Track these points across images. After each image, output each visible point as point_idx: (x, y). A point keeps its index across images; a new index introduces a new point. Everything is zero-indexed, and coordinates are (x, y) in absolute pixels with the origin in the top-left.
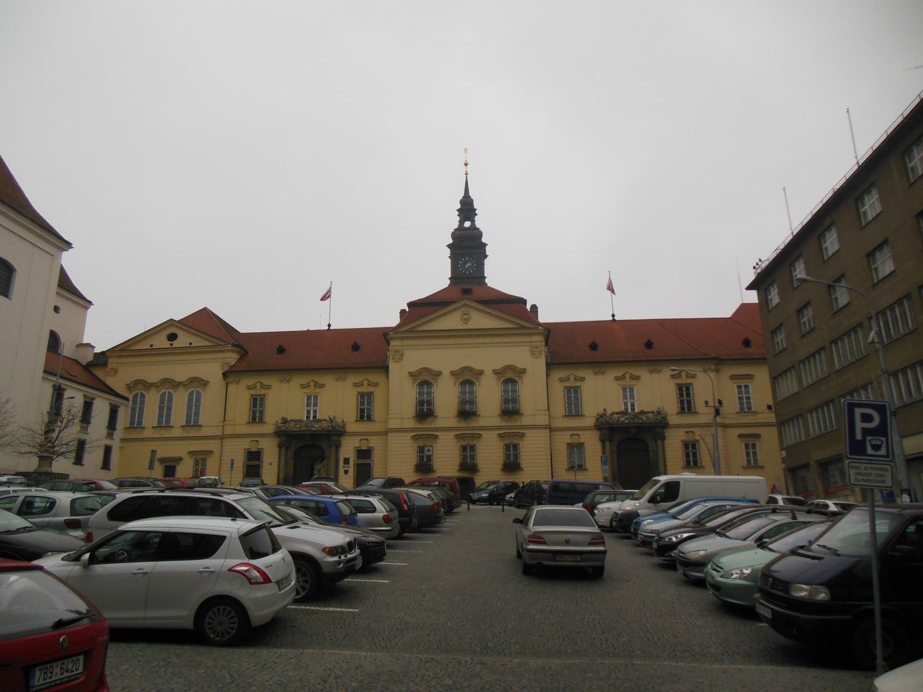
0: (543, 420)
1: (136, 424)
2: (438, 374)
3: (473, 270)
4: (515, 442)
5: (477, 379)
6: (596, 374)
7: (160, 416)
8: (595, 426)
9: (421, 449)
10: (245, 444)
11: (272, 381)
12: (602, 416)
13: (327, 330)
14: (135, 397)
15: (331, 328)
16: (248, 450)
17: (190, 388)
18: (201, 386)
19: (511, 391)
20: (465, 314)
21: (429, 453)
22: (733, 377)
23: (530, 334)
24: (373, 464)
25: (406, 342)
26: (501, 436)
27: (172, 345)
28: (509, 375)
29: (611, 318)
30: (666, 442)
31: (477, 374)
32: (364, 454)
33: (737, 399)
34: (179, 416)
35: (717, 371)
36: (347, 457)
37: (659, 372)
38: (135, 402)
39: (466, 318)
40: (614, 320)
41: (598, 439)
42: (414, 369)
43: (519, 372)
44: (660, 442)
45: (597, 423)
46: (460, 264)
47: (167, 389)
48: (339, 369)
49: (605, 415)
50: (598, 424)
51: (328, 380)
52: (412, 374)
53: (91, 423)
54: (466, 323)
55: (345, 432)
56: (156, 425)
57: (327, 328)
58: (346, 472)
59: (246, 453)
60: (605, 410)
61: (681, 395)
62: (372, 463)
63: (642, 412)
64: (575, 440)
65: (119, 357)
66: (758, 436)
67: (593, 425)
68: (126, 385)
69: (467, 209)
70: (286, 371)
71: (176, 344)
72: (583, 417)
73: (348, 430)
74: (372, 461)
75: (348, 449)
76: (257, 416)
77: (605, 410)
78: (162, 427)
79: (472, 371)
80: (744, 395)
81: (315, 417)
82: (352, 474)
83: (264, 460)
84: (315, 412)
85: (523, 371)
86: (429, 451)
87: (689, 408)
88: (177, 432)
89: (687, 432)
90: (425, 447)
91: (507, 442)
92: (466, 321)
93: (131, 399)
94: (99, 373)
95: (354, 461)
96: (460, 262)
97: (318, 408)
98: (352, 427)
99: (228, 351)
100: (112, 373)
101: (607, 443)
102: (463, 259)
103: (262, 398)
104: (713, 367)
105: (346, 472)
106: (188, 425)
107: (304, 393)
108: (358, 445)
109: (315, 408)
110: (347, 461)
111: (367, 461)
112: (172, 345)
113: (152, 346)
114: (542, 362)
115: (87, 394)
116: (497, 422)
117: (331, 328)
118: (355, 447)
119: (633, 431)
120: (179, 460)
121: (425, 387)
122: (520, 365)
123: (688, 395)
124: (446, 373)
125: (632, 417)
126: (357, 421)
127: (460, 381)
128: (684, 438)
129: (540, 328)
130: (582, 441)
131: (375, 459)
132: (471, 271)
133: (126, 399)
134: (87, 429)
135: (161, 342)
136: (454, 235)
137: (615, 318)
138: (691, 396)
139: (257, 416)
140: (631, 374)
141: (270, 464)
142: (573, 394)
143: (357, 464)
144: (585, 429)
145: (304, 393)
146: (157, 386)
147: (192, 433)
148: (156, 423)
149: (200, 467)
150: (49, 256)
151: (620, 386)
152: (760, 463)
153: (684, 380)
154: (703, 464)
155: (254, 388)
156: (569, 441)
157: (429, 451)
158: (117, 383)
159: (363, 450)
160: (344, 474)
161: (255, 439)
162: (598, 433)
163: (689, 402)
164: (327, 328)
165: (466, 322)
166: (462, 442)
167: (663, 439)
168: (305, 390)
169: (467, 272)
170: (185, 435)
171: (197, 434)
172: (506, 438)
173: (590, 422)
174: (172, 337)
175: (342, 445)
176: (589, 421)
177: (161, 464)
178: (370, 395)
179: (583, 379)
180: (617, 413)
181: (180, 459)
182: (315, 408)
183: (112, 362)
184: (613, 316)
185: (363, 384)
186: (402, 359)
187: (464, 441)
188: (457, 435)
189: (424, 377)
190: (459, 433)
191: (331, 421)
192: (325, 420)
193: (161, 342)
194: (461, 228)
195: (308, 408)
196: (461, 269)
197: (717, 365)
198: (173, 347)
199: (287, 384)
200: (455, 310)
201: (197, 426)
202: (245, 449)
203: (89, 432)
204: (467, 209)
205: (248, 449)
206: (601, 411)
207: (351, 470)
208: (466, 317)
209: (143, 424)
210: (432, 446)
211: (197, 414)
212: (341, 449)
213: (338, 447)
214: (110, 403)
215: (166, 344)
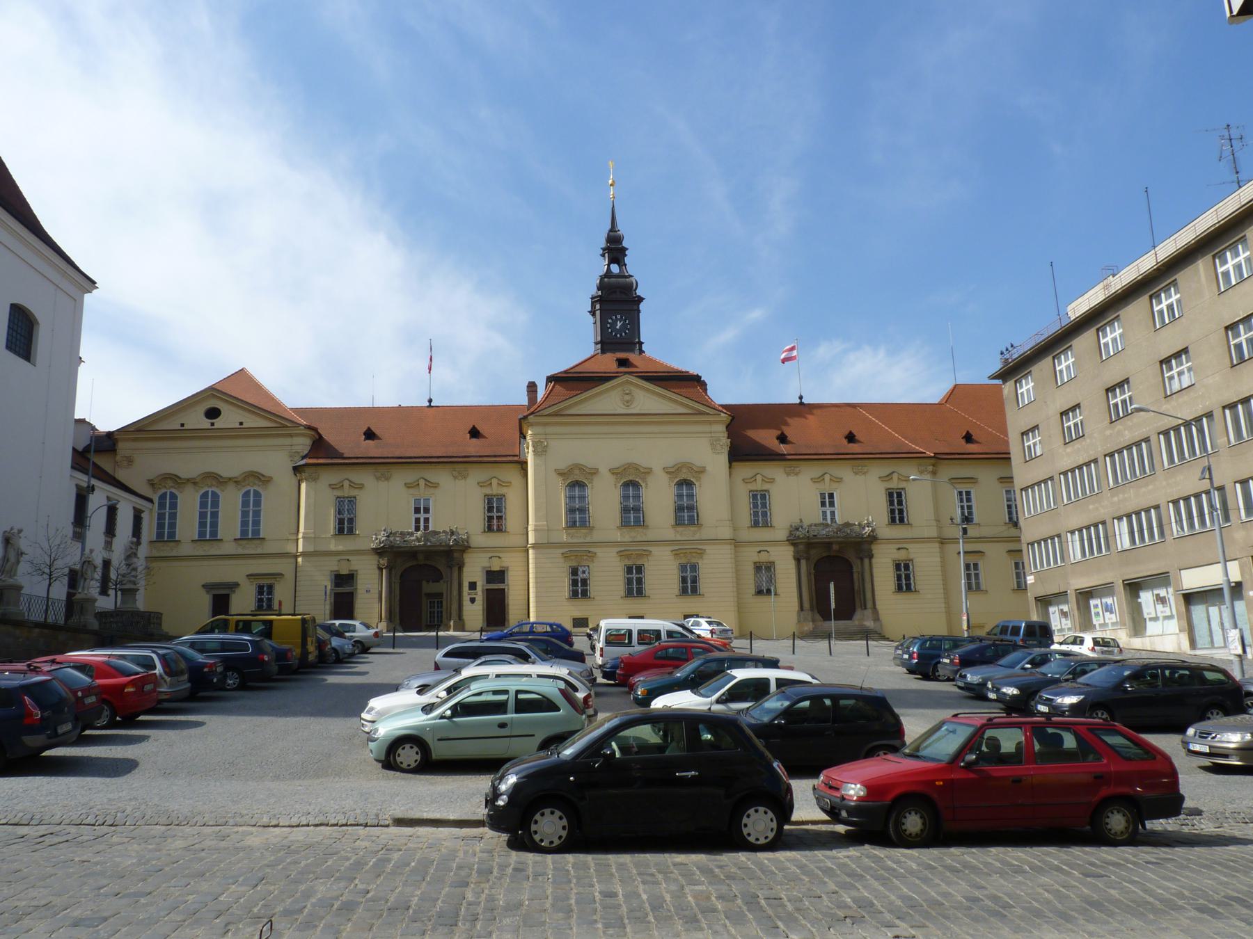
0: (726, 533)
1: (167, 534)
2: (595, 472)
3: (626, 333)
4: (693, 561)
5: (644, 480)
6: (788, 474)
7: (202, 524)
8: (787, 540)
9: (574, 571)
10: (332, 565)
11: (365, 477)
13: (428, 407)
14: (163, 497)
15: (432, 404)
16: (336, 573)
17: (244, 486)
18: (260, 483)
19: (687, 496)
20: (627, 394)
21: (585, 575)
22: (954, 481)
23: (710, 423)
24: (508, 589)
25: (550, 429)
26: (676, 554)
27: (213, 424)
28: (683, 476)
29: (798, 401)
30: (874, 561)
31: (643, 473)
32: (496, 576)
33: (1006, 507)
34: (230, 524)
35: (934, 473)
36: (473, 580)
37: (865, 473)
38: (162, 505)
39: (628, 399)
40: (801, 404)
42: (563, 465)
43: (696, 472)
44: (866, 561)
46: (610, 323)
47: (210, 487)
48: (457, 463)
49: (802, 527)
50: (791, 538)
51: (442, 477)
52: (561, 473)
53: (115, 536)
54: (628, 406)
55: (470, 547)
56: (197, 538)
57: (428, 404)
58: (473, 600)
59: (333, 577)
60: (801, 521)
61: (891, 503)
62: (506, 588)
63: (847, 525)
64: (764, 558)
65: (135, 440)
67: (785, 539)
68: (149, 480)
69: (615, 250)
70: (383, 465)
71: (219, 423)
72: (771, 529)
73: (472, 546)
74: (508, 585)
75: (474, 570)
76: (345, 526)
77: (801, 521)
78: (207, 540)
79: (637, 469)
80: (965, 504)
81: (426, 528)
82: (481, 603)
83: (359, 587)
84: (427, 520)
85: (702, 471)
86: (584, 572)
87: (901, 520)
88: (229, 548)
89: (899, 549)
90: (579, 568)
91: (684, 561)
92: (628, 403)
93: (156, 500)
94: (104, 462)
95: (483, 586)
96: (610, 321)
97: (430, 516)
98: (479, 539)
99: (297, 435)
100: (125, 463)
101: (803, 562)
102: (614, 317)
103: (352, 501)
104: (930, 468)
105: (473, 600)
106: (244, 537)
108: (487, 565)
109: (427, 516)
110: (473, 586)
111: (501, 586)
112: (213, 424)
113: (182, 425)
114: (723, 458)
115: (110, 495)
116: (670, 534)
117: (432, 404)
118: (484, 568)
119: (835, 547)
120: (234, 586)
121: (631, 488)
122: (697, 461)
123: (900, 503)
124: (604, 470)
126: (485, 532)
127: (622, 482)
129: (722, 414)
130: (771, 559)
131: (510, 582)
132: (623, 334)
133: (151, 501)
134: (111, 544)
135: (197, 420)
136: (601, 287)
137: (803, 401)
138: (904, 503)
139: (345, 526)
141: (368, 591)
142: (759, 503)
143: (487, 590)
144: (775, 543)
146: (195, 484)
147: (251, 549)
148: (197, 535)
149: (265, 596)
151: (817, 490)
152: (983, 587)
153: (894, 484)
154: (918, 588)
155: (415, 486)
156: (757, 559)
157: (584, 572)
158: (133, 476)
159: (494, 571)
160: (469, 602)
161: (347, 557)
162: (791, 549)
163: (901, 512)
164: (428, 404)
165: (628, 404)
166: (626, 561)
167: (871, 557)
168: (411, 491)
169: (618, 335)
170: (240, 551)
171: (259, 551)
172: (682, 555)
173: (782, 534)
174: (213, 413)
175: (466, 565)
176: (780, 532)
177: (208, 592)
178: (501, 498)
180: (815, 525)
181: (236, 585)
182: (427, 516)
183: (121, 446)
184: (801, 398)
185: (491, 483)
186: (546, 451)
187: (629, 560)
188: (621, 551)
189: (575, 477)
190: (623, 549)
191: (452, 533)
192: (444, 532)
193: (197, 420)
194: (608, 274)
195: (418, 516)
196: (610, 331)
197: (934, 465)
198: (215, 427)
199: (386, 482)
200: (613, 388)
201: (257, 537)
202: (331, 571)
203: (113, 548)
204: (615, 250)
205: (337, 571)
206: (796, 522)
207: (479, 595)
208: (627, 398)
209: (177, 536)
210: (588, 566)
211: (257, 523)
212: (465, 569)
213: (461, 567)
214: (134, 508)
215: (206, 423)
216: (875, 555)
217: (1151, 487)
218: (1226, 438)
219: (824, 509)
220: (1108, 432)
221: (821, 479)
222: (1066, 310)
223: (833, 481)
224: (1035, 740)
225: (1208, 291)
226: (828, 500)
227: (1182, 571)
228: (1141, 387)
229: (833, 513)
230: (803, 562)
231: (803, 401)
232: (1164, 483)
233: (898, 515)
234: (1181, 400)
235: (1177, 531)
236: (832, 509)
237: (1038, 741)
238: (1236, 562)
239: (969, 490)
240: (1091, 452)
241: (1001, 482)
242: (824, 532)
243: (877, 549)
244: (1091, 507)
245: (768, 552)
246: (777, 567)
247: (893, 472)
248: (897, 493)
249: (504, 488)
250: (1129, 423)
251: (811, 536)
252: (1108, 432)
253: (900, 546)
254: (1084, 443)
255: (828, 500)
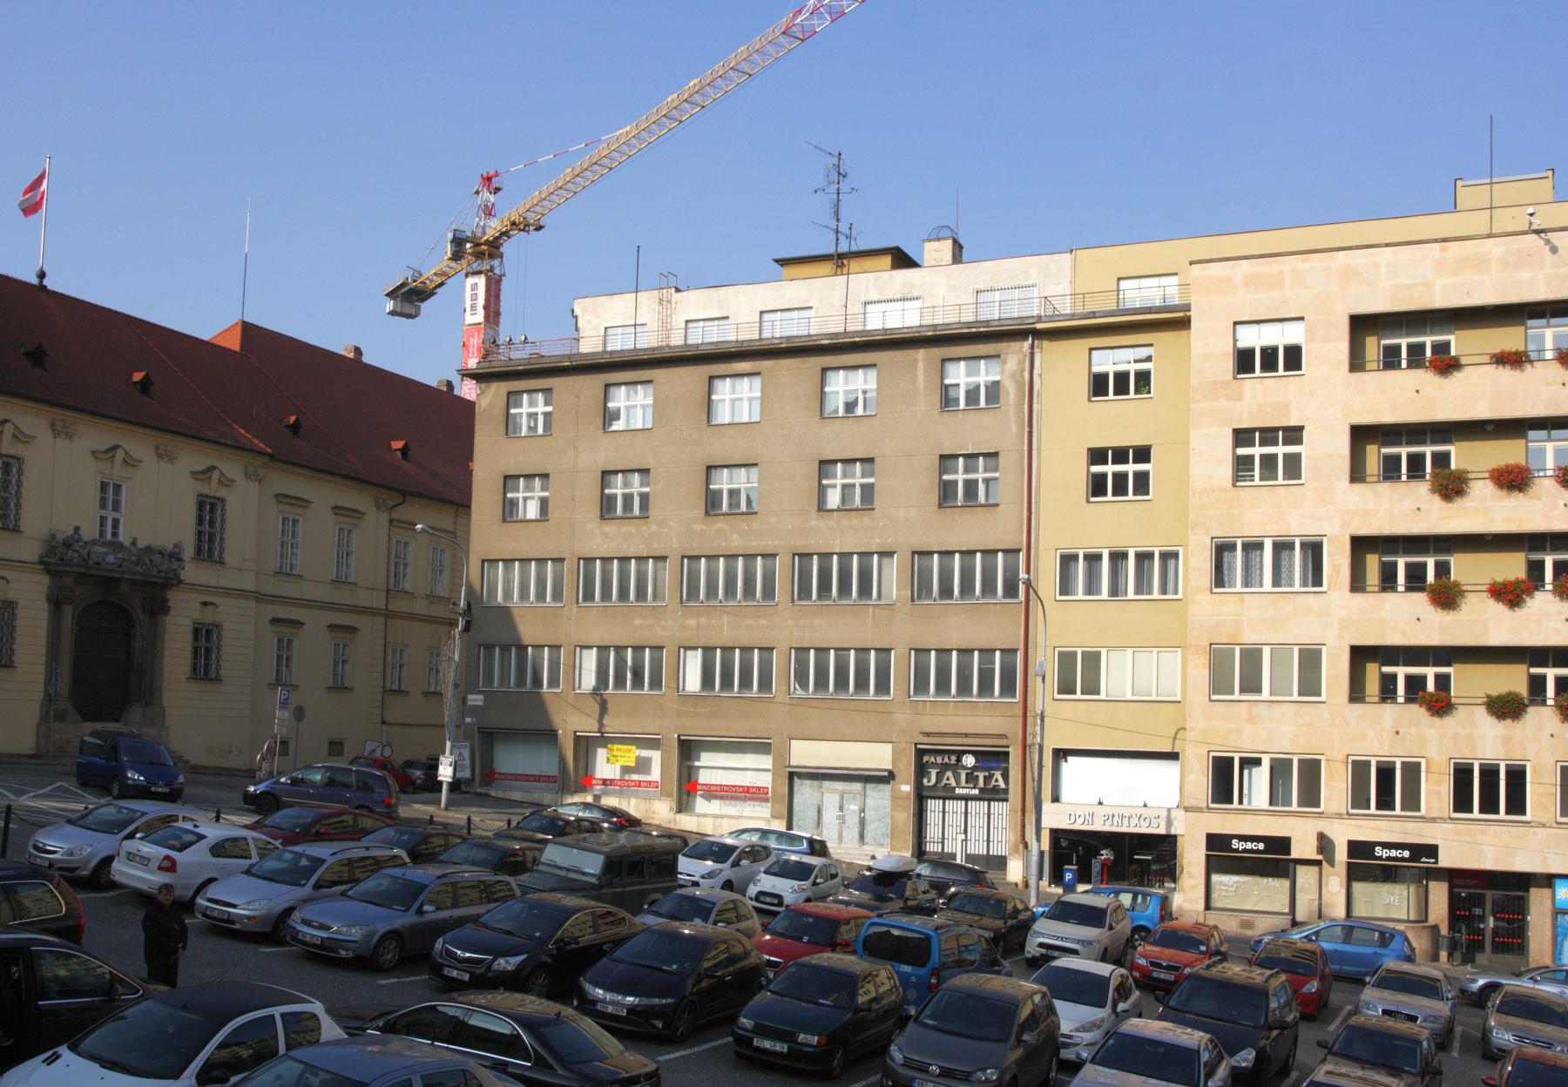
8: (41, 562)
12: (67, 544)
22: (279, 497)
35: (260, 480)
40: (43, 288)
41: (43, 597)
45: (46, 556)
61: (200, 521)
66: (297, 624)
77: (77, 529)
89: (205, 604)
107: (100, 472)
125: (134, 558)
128: (197, 616)
130: (11, 596)
137: (45, 282)
140: (126, 452)
144: (19, 564)
145: (100, 472)
150: (995, 360)
173: (29, 549)
179: (131, 462)
184: (42, 275)
216: (172, 611)
217: (763, 622)
218: (909, 592)
219: (104, 513)
220: (698, 527)
221: (207, 475)
222: (573, 304)
223: (19, 439)
224: (522, 957)
225: (927, 403)
226: (109, 494)
227: (792, 741)
228: (777, 484)
229: (116, 523)
230: (68, 611)
231: (45, 282)
232: (789, 622)
233: (209, 544)
234: (844, 523)
235: (795, 689)
236: (115, 515)
237: (523, 961)
238: (890, 746)
239: (296, 517)
240: (655, 545)
241: (336, 514)
242: (111, 559)
243: (176, 598)
244: (638, 622)
245: (8, 582)
246: (19, 612)
247: (6, 421)
248: (114, 484)
249: (20, 445)
250: (744, 526)
251: (92, 563)
252: (698, 527)
253: (209, 599)
254: (644, 528)
255: (109, 494)
